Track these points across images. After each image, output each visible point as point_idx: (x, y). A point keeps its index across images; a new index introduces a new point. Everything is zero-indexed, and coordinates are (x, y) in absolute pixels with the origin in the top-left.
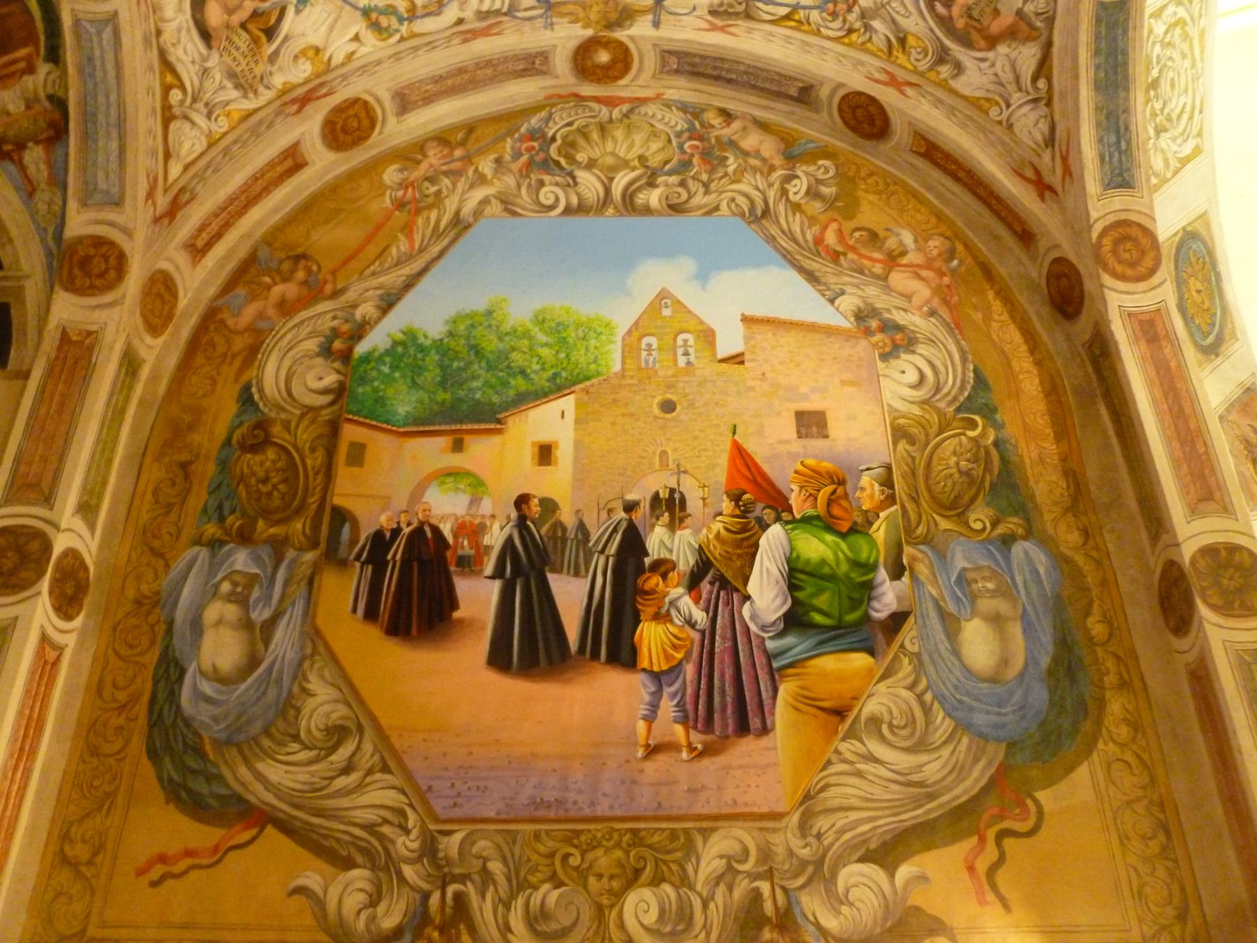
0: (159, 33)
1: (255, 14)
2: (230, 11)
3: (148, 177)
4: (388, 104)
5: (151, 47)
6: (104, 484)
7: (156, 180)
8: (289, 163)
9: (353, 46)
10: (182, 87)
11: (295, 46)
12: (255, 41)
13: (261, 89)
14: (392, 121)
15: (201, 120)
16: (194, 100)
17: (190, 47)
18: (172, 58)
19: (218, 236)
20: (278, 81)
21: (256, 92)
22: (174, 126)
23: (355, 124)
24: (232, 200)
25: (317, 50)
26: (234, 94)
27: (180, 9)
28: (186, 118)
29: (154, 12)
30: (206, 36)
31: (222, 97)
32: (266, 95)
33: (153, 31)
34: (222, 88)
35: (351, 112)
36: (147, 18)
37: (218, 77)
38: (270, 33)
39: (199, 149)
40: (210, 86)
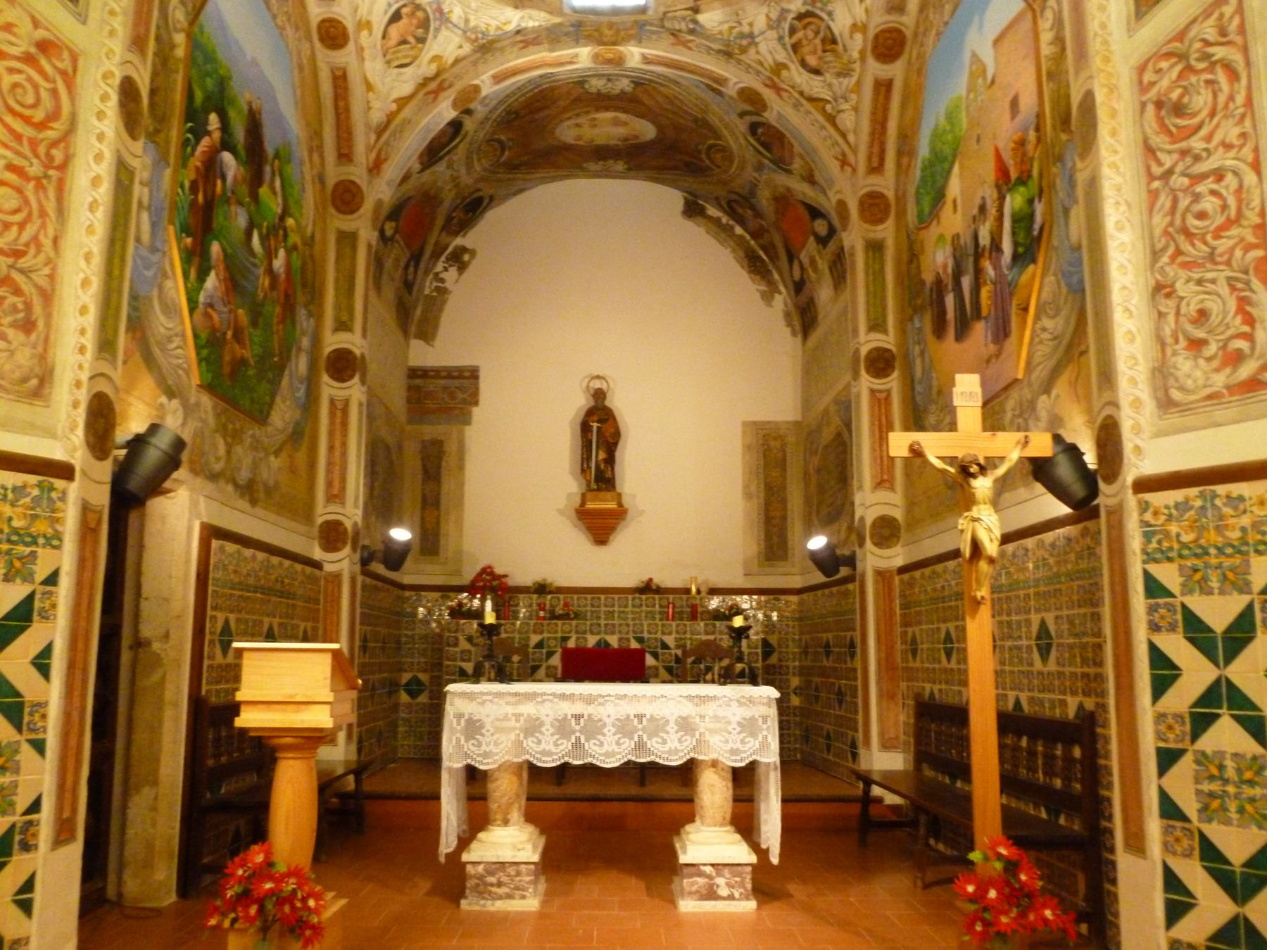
0: (801, 93)
1: (823, 41)
2: (815, 52)
3: (837, 159)
4: (891, 18)
5: (802, 105)
6: (884, 308)
7: (844, 154)
8: (883, 89)
9: (864, 6)
10: (828, 102)
11: (846, 33)
12: (833, 51)
13: (854, 66)
14: (904, 19)
15: (845, 106)
16: (836, 100)
17: (816, 83)
18: (815, 96)
19: (882, 152)
20: (856, 55)
21: (853, 70)
22: (838, 121)
23: (890, 42)
24: (872, 133)
25: (854, 25)
26: (845, 81)
27: (800, 74)
28: (839, 112)
29: (793, 87)
30: (817, 72)
31: (844, 87)
32: (857, 66)
33: (797, 95)
34: (840, 83)
35: (881, 41)
36: (791, 96)
37: (835, 81)
38: (834, 41)
39: (853, 118)
40: (836, 88)
